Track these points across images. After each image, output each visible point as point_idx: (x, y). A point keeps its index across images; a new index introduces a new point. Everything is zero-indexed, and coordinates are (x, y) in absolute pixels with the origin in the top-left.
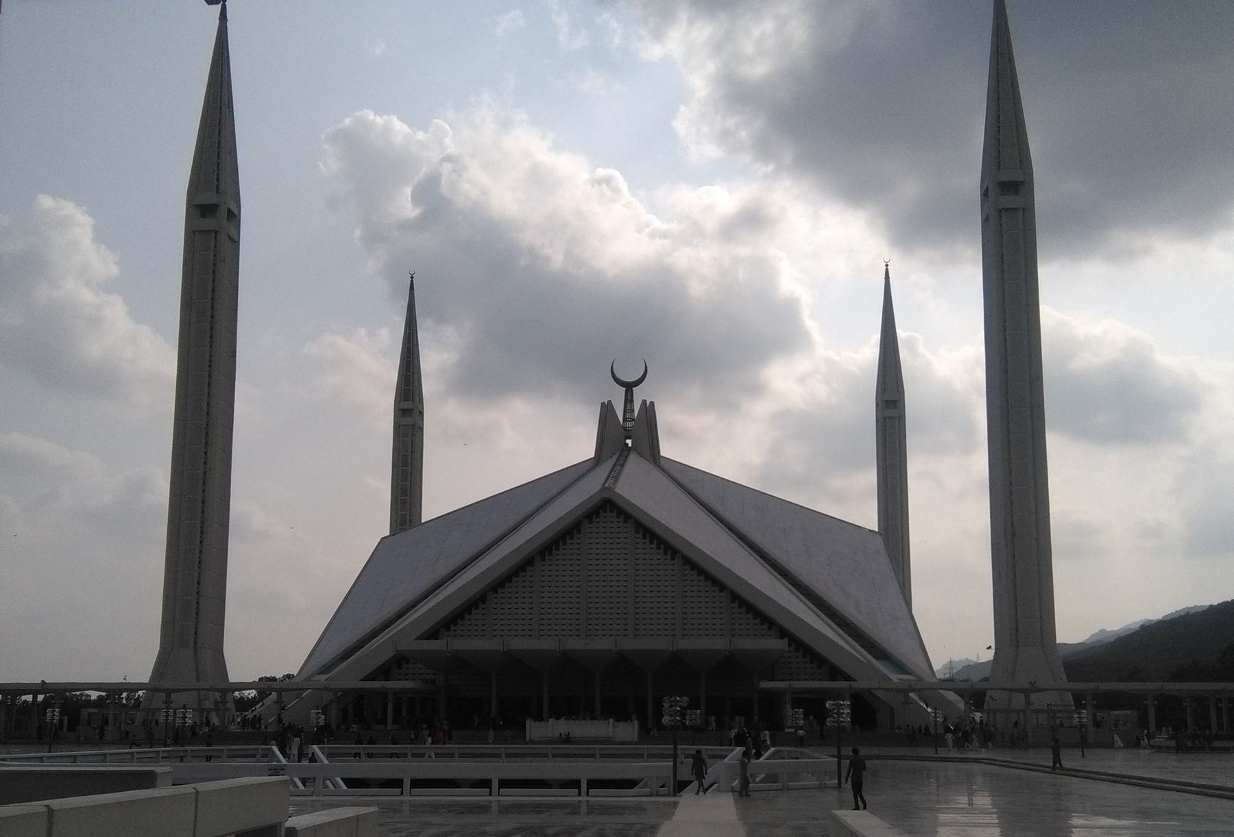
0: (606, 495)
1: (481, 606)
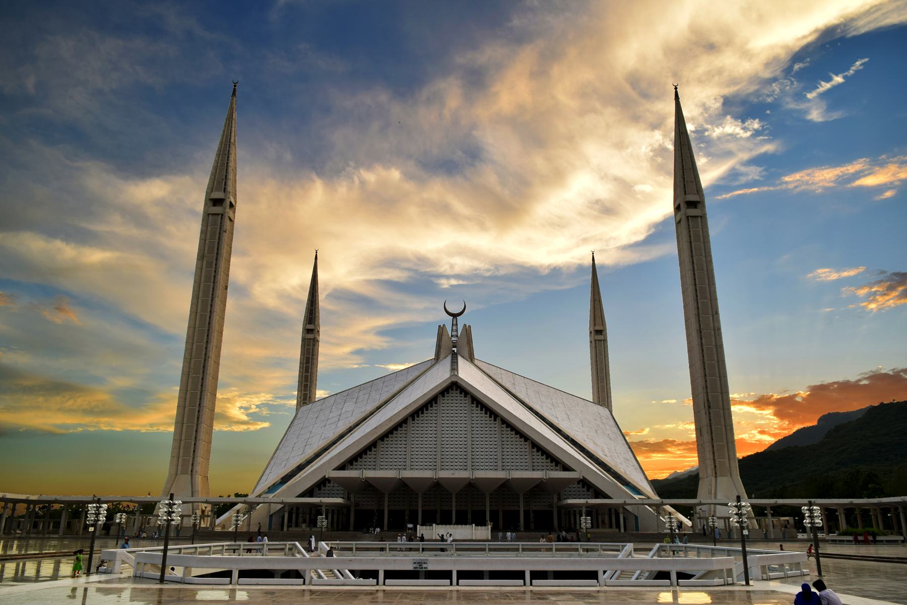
0: (454, 379)
1: (373, 449)
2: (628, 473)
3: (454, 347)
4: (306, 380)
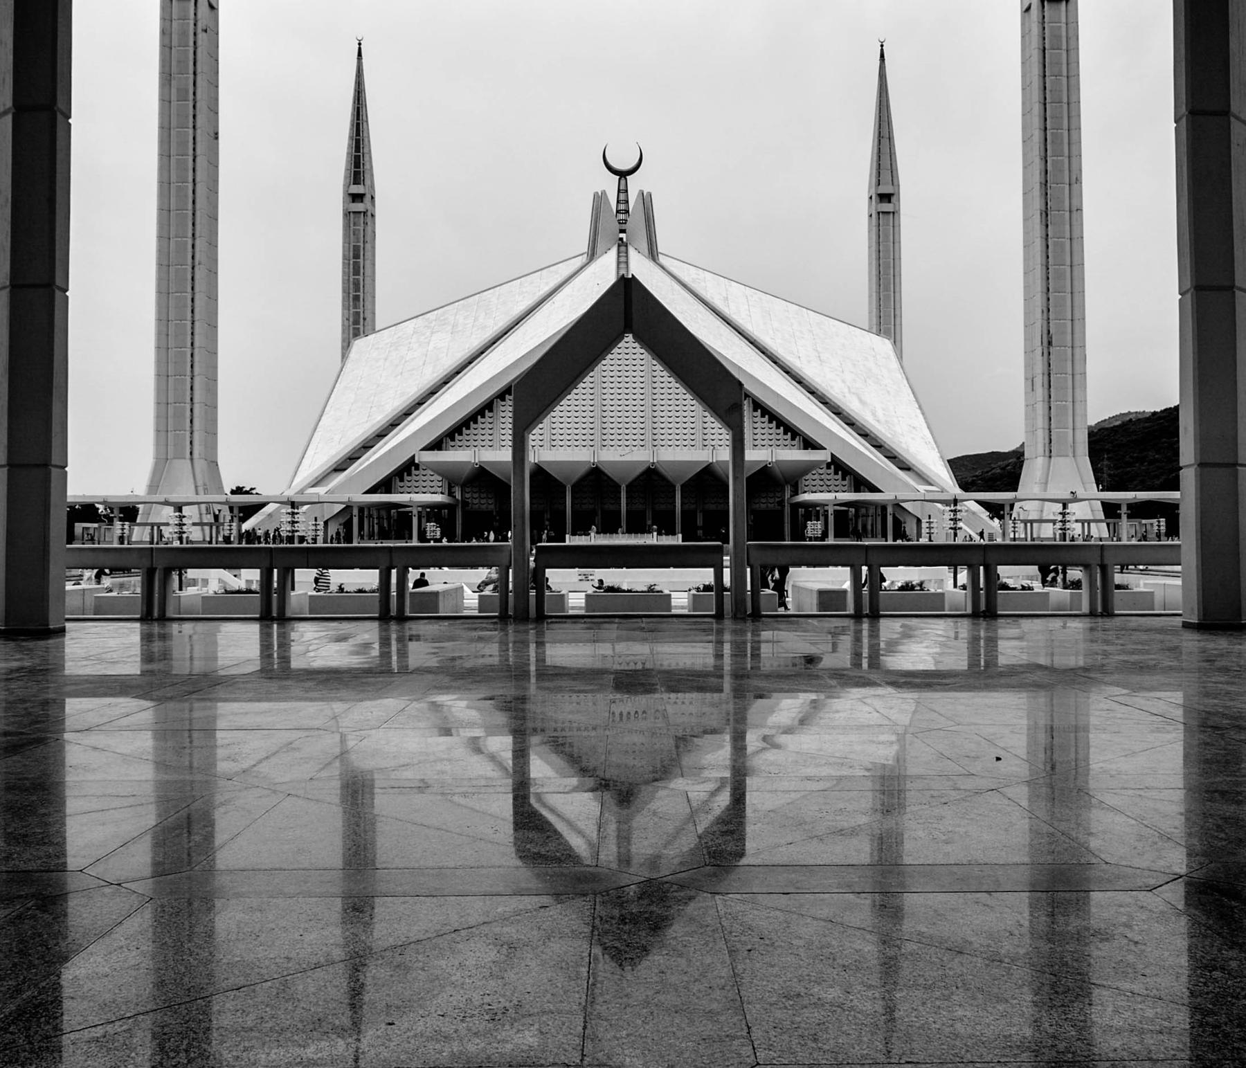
2: (912, 450)
3: (623, 231)
4: (357, 289)
